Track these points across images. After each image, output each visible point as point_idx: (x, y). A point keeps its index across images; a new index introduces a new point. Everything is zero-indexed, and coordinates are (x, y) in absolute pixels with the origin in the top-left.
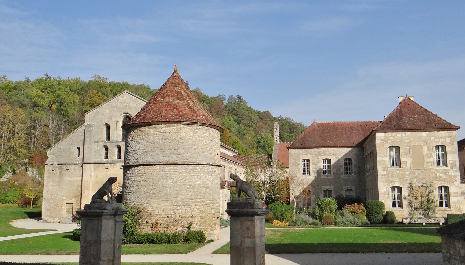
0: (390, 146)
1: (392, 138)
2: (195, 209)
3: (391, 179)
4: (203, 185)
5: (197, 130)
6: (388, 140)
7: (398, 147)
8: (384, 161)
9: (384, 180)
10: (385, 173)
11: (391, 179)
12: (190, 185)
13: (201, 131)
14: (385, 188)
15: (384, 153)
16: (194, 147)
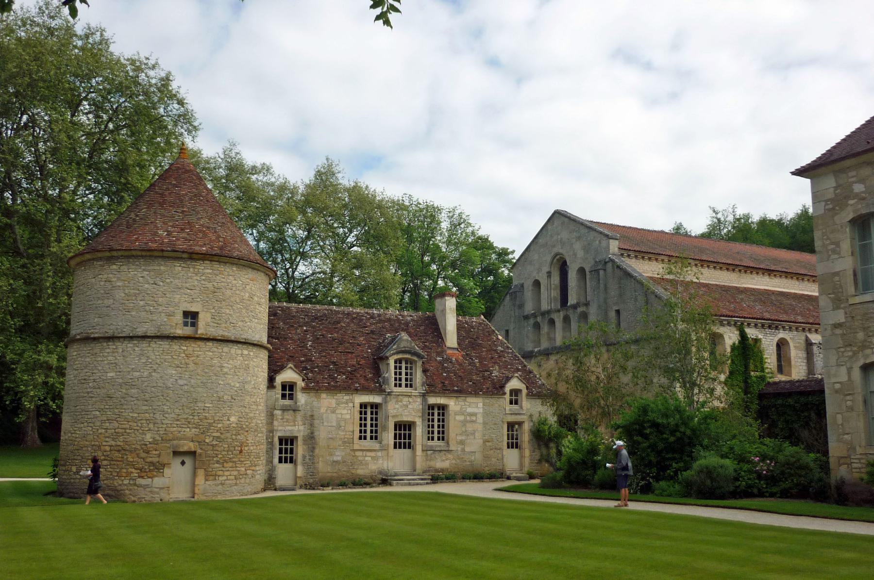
0: (851, 216)
1: (858, 188)
2: (100, 431)
3: (861, 335)
4: (121, 381)
5: (114, 267)
6: (847, 198)
7: (557, 214)
8: (837, 274)
9: (841, 343)
10: (840, 316)
11: (861, 335)
12: (94, 381)
13: (122, 268)
14: (843, 370)
15: (837, 244)
16: (106, 301)
